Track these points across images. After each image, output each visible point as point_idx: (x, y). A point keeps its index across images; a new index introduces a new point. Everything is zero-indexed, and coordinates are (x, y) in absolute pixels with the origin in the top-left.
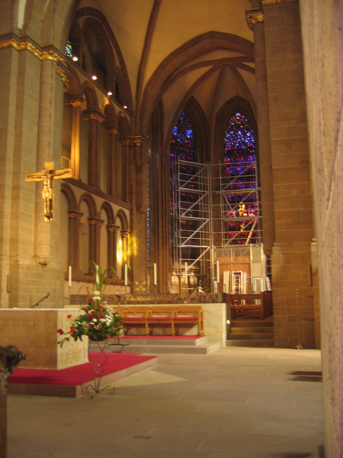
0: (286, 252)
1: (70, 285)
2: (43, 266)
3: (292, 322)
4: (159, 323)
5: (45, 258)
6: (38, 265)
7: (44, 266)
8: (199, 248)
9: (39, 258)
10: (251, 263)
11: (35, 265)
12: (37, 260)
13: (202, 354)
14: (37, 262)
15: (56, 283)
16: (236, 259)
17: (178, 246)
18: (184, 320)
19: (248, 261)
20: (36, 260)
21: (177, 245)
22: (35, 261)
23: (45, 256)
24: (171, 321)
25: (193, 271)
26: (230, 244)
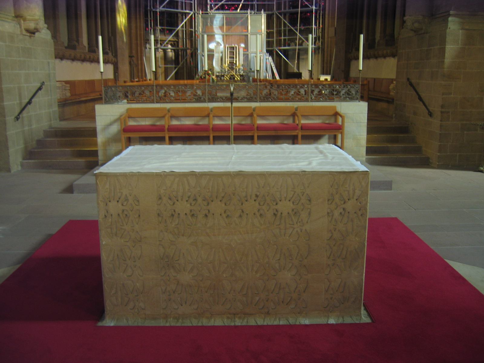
0: (467, 27)
1: (102, 70)
2: (31, 35)
3: (465, 132)
4: (277, 134)
5: (36, 20)
6: (24, 32)
7: (33, 35)
8: (177, 13)
9: (25, 20)
10: (249, 36)
11: (19, 33)
12: (23, 25)
13: (384, 190)
14: (23, 28)
15: (49, 63)
16: (229, 30)
17: (154, 10)
18: (314, 130)
19: (245, 32)
20: (20, 24)
21: (152, 8)
22: (18, 26)
23: (37, 17)
24: (297, 131)
25: (170, 43)
26: (218, 9)
